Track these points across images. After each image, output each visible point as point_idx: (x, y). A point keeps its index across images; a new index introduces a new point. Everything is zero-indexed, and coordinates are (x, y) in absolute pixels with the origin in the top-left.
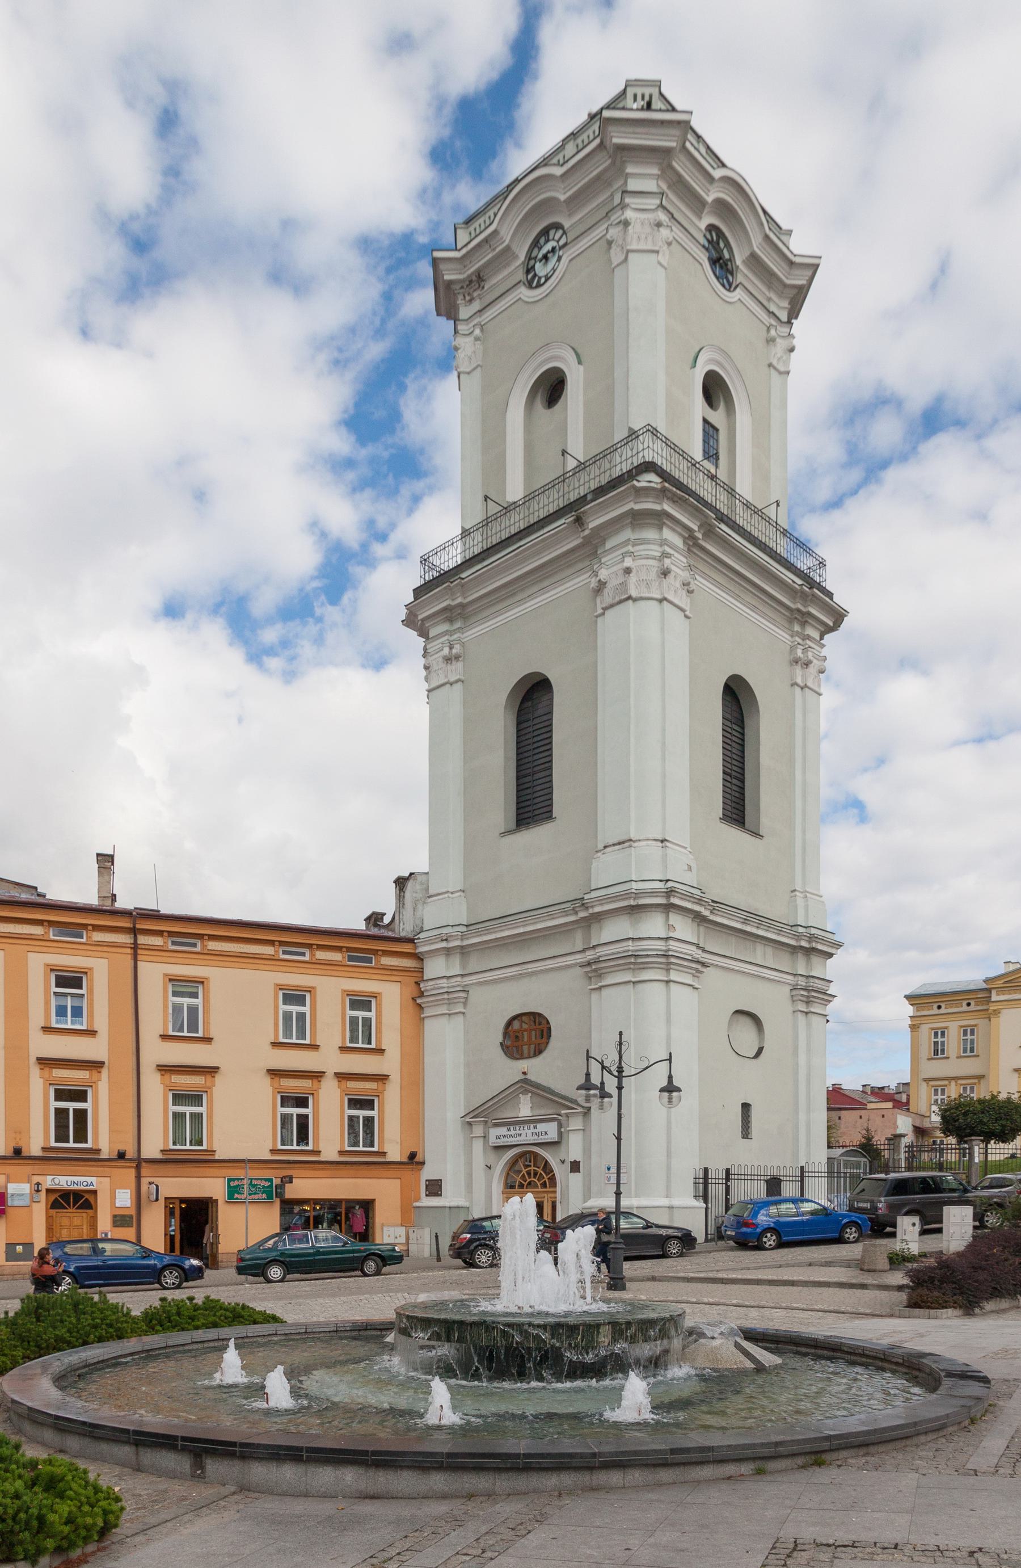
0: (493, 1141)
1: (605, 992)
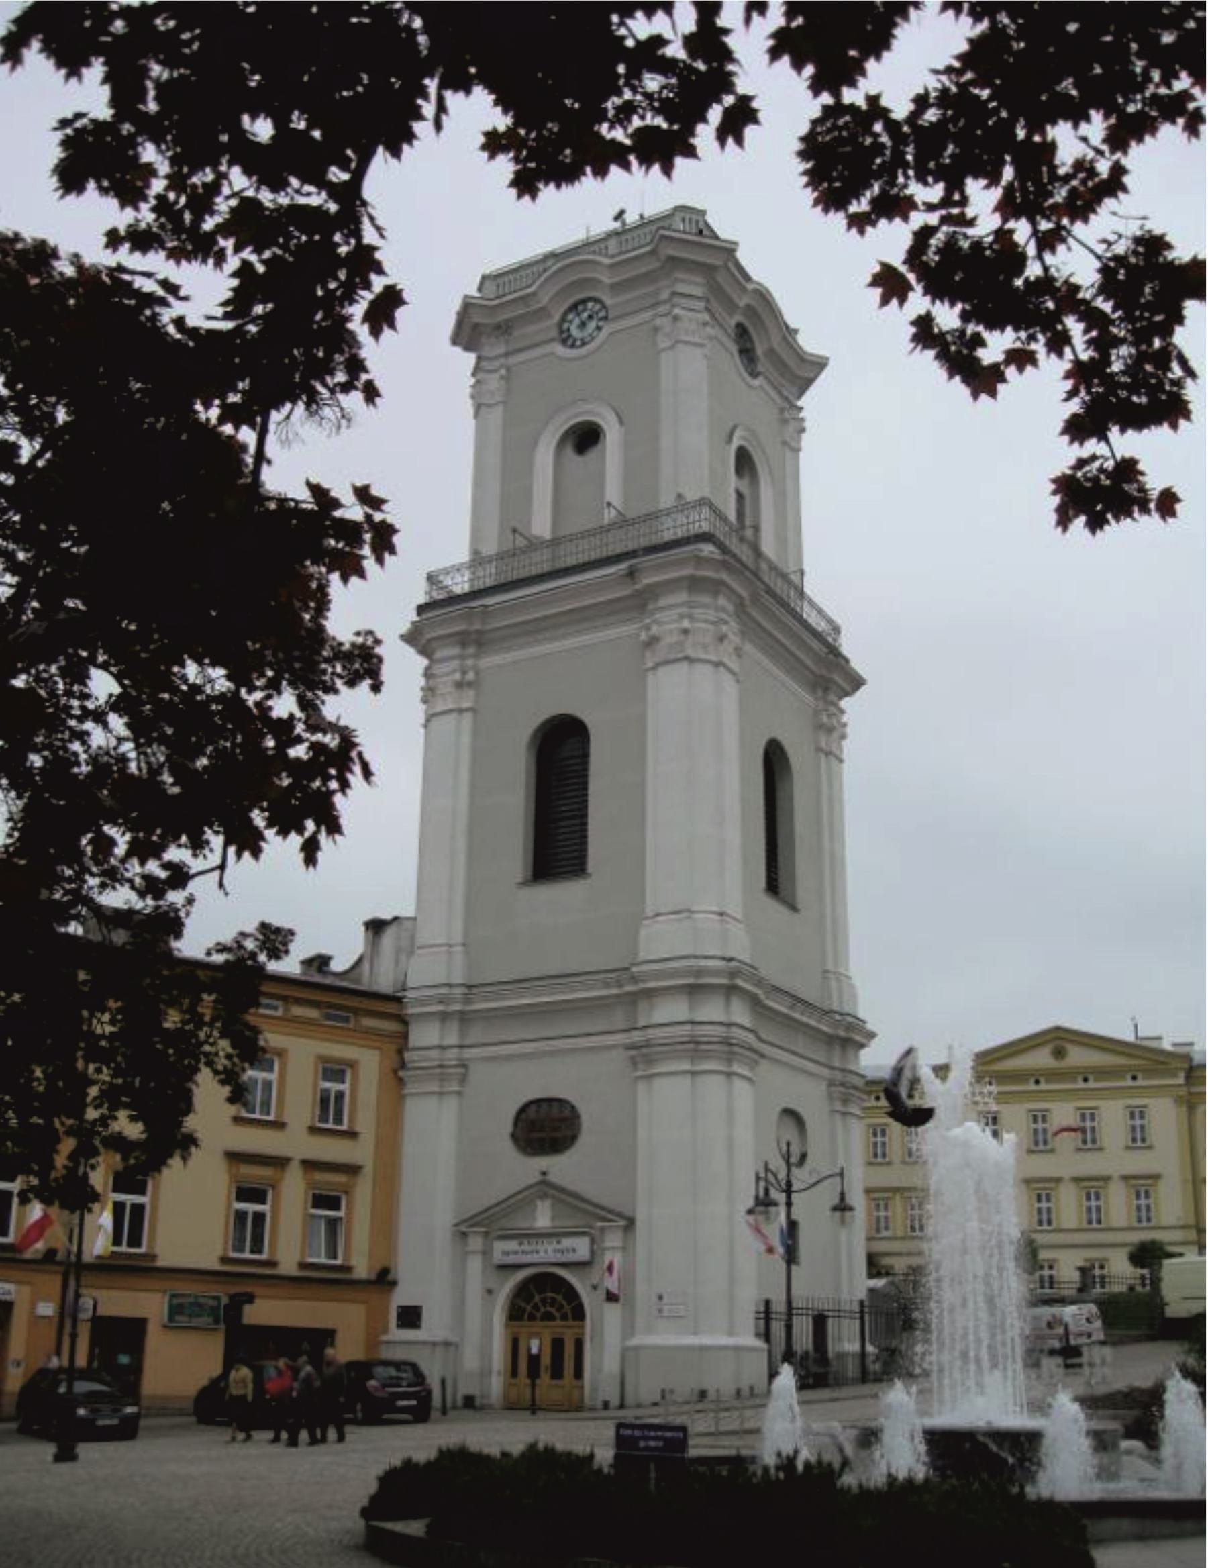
0: (498, 1257)
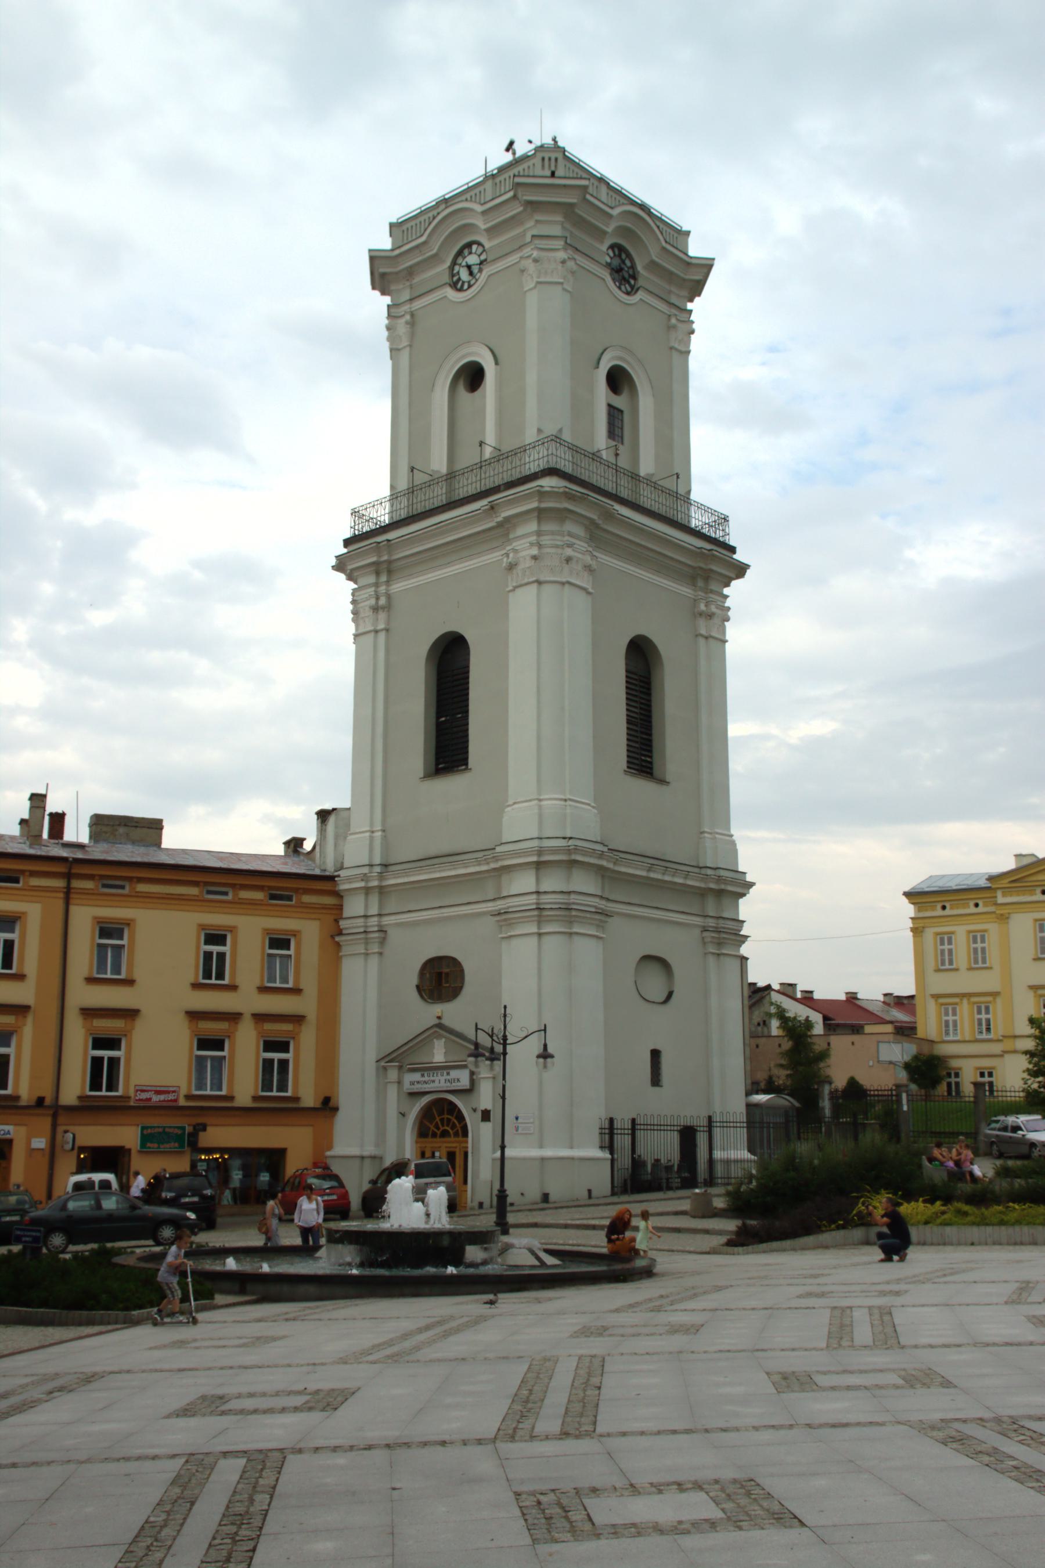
0: (407, 1087)
1: (515, 942)
